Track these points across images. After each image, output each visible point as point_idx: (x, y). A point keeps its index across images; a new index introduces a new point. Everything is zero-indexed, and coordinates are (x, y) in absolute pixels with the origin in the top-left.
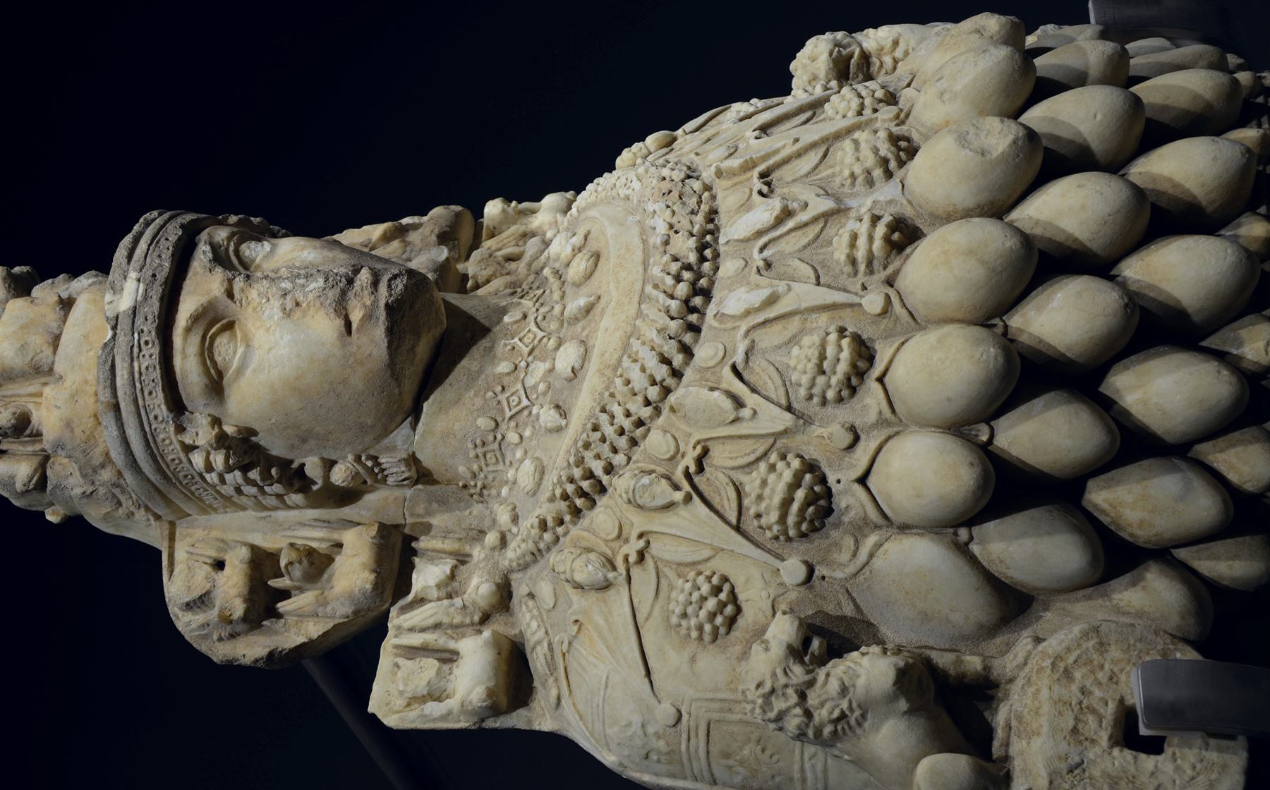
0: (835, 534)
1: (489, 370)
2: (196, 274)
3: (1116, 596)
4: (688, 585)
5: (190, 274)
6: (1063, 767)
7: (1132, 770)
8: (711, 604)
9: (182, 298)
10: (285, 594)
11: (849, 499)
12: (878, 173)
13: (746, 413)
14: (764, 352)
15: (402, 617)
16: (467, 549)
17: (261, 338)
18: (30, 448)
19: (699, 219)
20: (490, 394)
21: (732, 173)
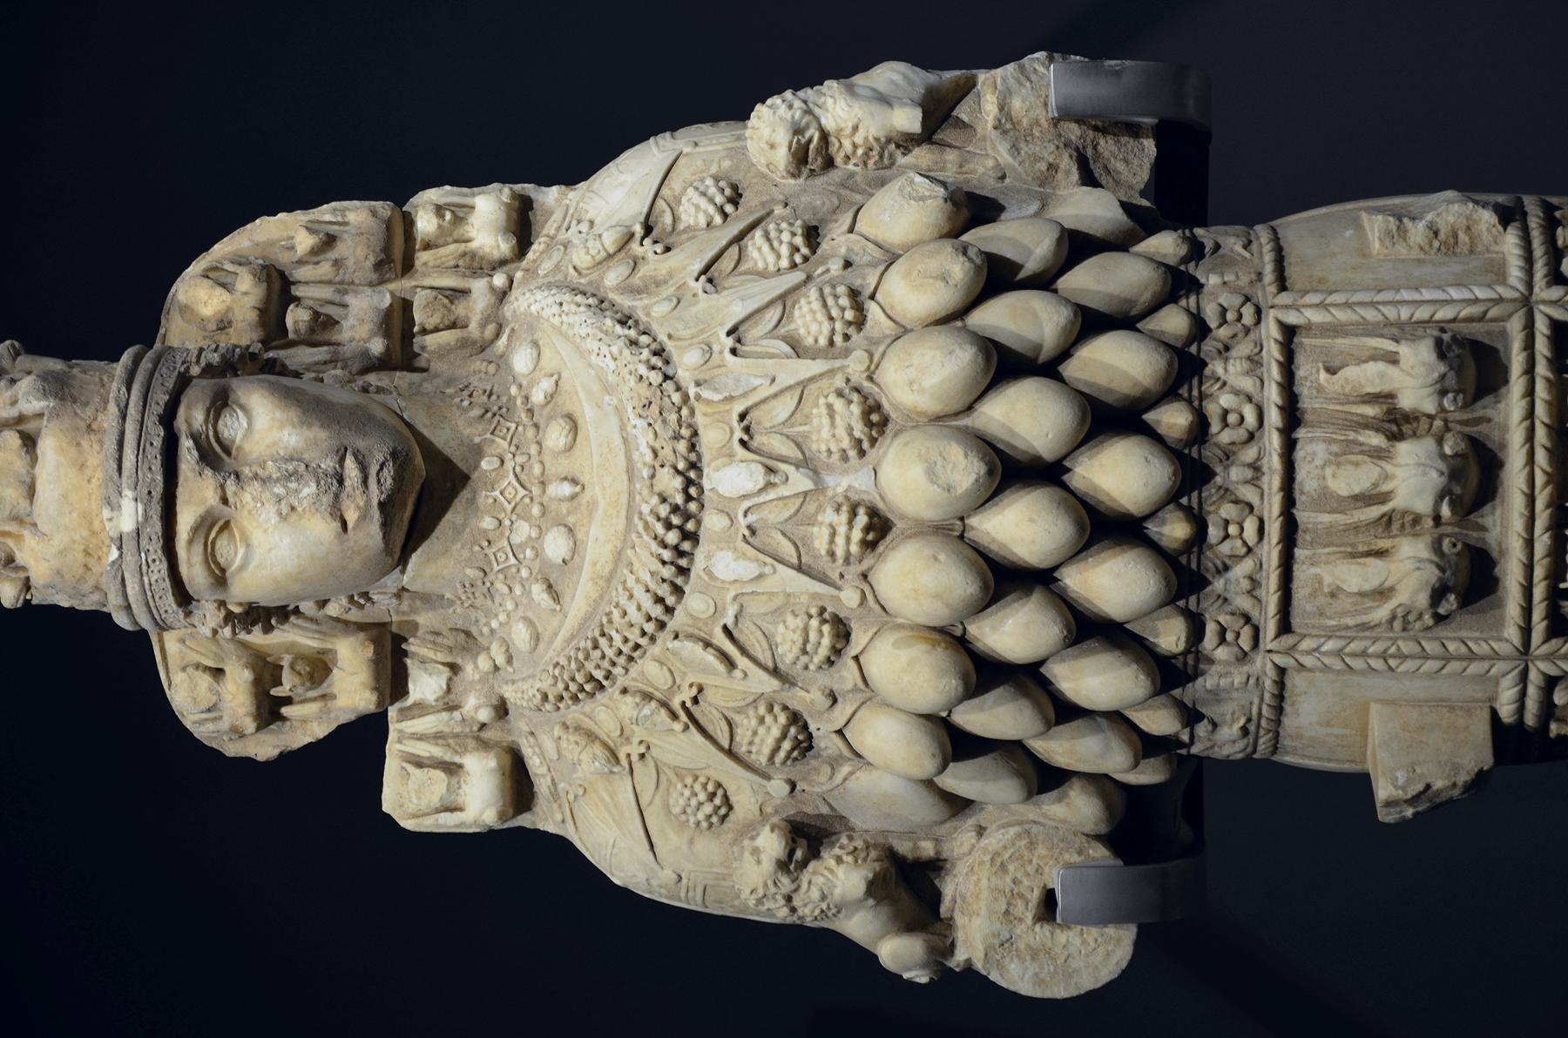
0: (814, 763)
1: (473, 522)
2: (186, 480)
3: (1045, 808)
4: (687, 793)
5: (181, 480)
6: (997, 942)
7: (1049, 943)
8: (708, 809)
9: (178, 508)
10: (288, 701)
11: (826, 742)
12: (852, 453)
13: (738, 673)
14: (752, 615)
15: (404, 724)
16: (459, 661)
17: (257, 537)
18: (13, 575)
19: (682, 446)
20: (477, 548)
21: (709, 402)
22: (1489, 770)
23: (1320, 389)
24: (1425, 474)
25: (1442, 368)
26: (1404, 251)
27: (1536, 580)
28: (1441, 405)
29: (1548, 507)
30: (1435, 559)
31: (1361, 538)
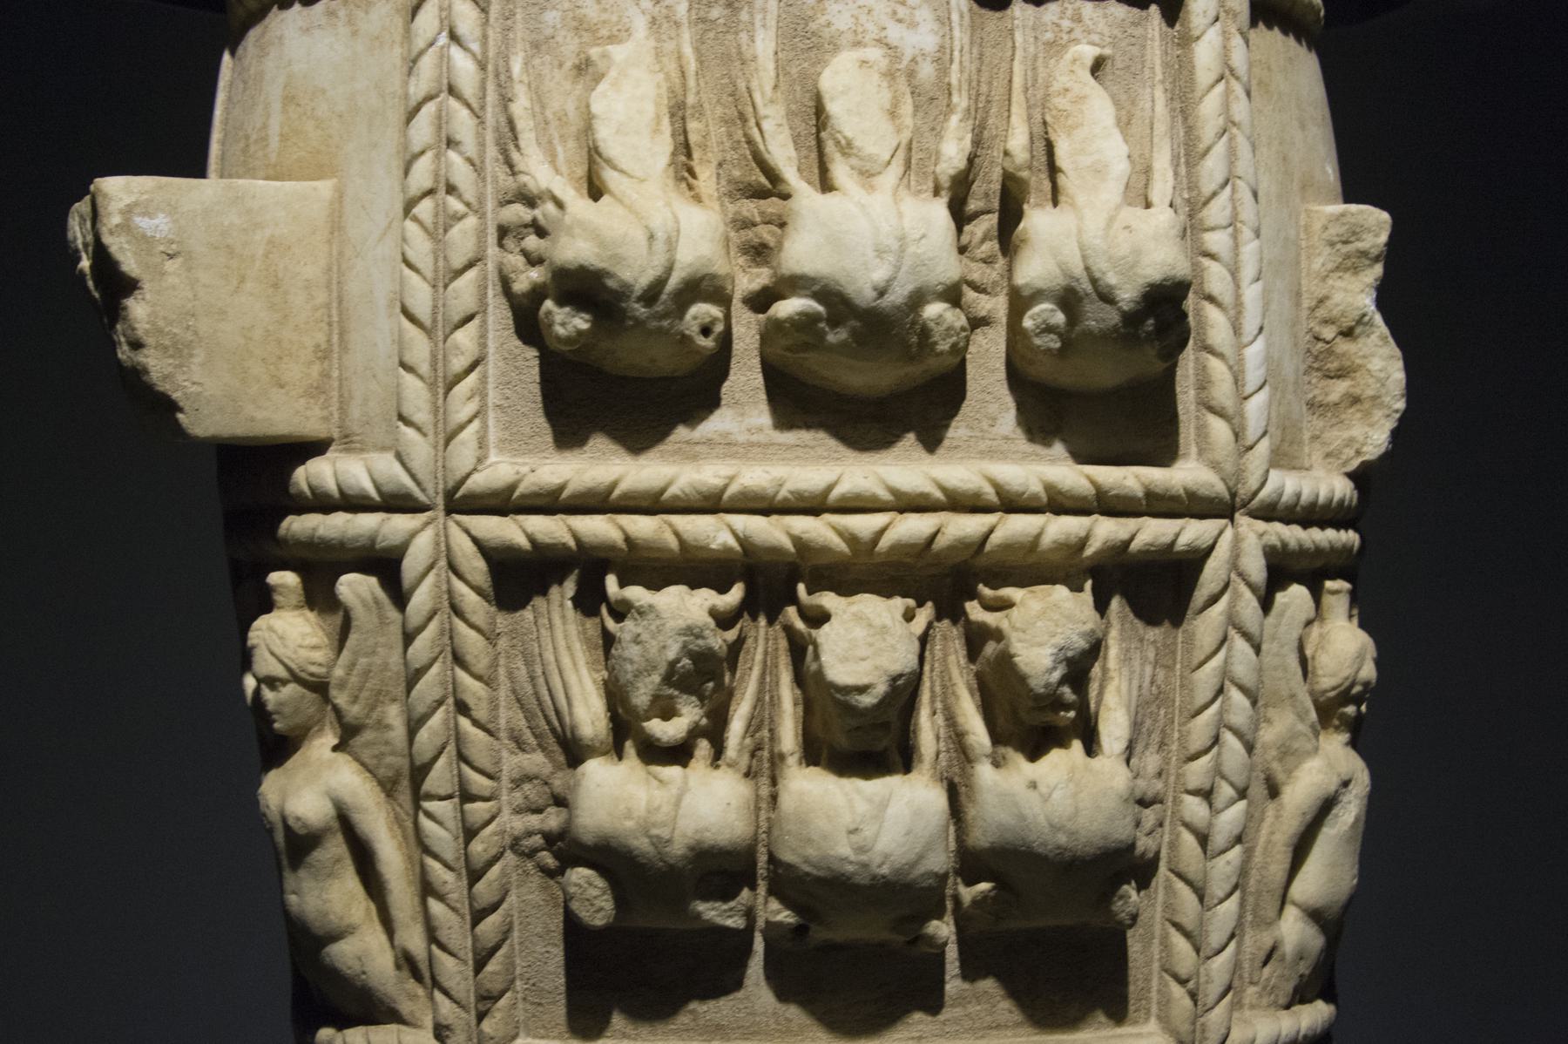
22: (178, 429)
23: (1055, 48)
24: (880, 252)
25: (1127, 295)
26: (1317, 264)
27: (627, 520)
28: (1037, 295)
29: (797, 541)
30: (673, 282)
31: (717, 132)
